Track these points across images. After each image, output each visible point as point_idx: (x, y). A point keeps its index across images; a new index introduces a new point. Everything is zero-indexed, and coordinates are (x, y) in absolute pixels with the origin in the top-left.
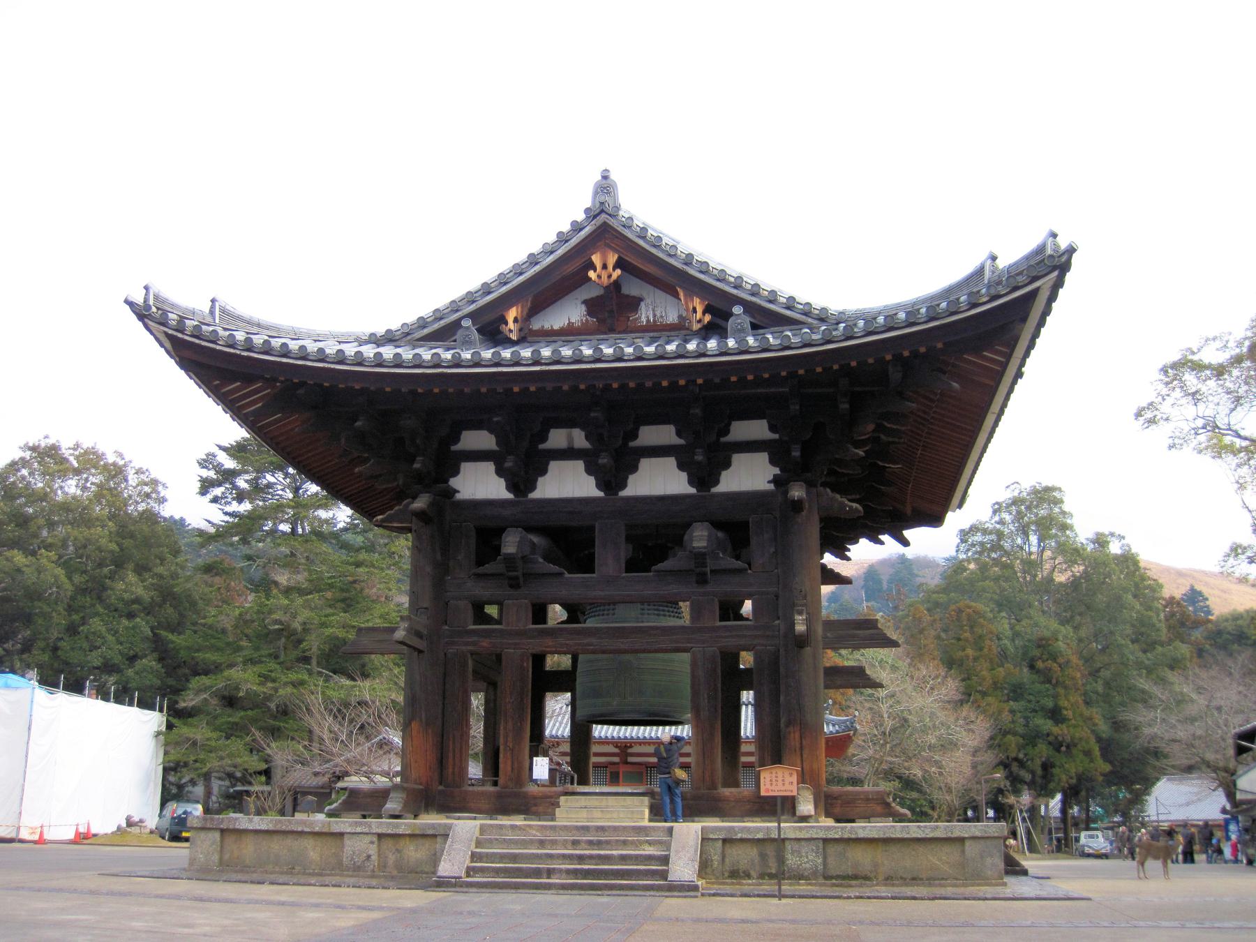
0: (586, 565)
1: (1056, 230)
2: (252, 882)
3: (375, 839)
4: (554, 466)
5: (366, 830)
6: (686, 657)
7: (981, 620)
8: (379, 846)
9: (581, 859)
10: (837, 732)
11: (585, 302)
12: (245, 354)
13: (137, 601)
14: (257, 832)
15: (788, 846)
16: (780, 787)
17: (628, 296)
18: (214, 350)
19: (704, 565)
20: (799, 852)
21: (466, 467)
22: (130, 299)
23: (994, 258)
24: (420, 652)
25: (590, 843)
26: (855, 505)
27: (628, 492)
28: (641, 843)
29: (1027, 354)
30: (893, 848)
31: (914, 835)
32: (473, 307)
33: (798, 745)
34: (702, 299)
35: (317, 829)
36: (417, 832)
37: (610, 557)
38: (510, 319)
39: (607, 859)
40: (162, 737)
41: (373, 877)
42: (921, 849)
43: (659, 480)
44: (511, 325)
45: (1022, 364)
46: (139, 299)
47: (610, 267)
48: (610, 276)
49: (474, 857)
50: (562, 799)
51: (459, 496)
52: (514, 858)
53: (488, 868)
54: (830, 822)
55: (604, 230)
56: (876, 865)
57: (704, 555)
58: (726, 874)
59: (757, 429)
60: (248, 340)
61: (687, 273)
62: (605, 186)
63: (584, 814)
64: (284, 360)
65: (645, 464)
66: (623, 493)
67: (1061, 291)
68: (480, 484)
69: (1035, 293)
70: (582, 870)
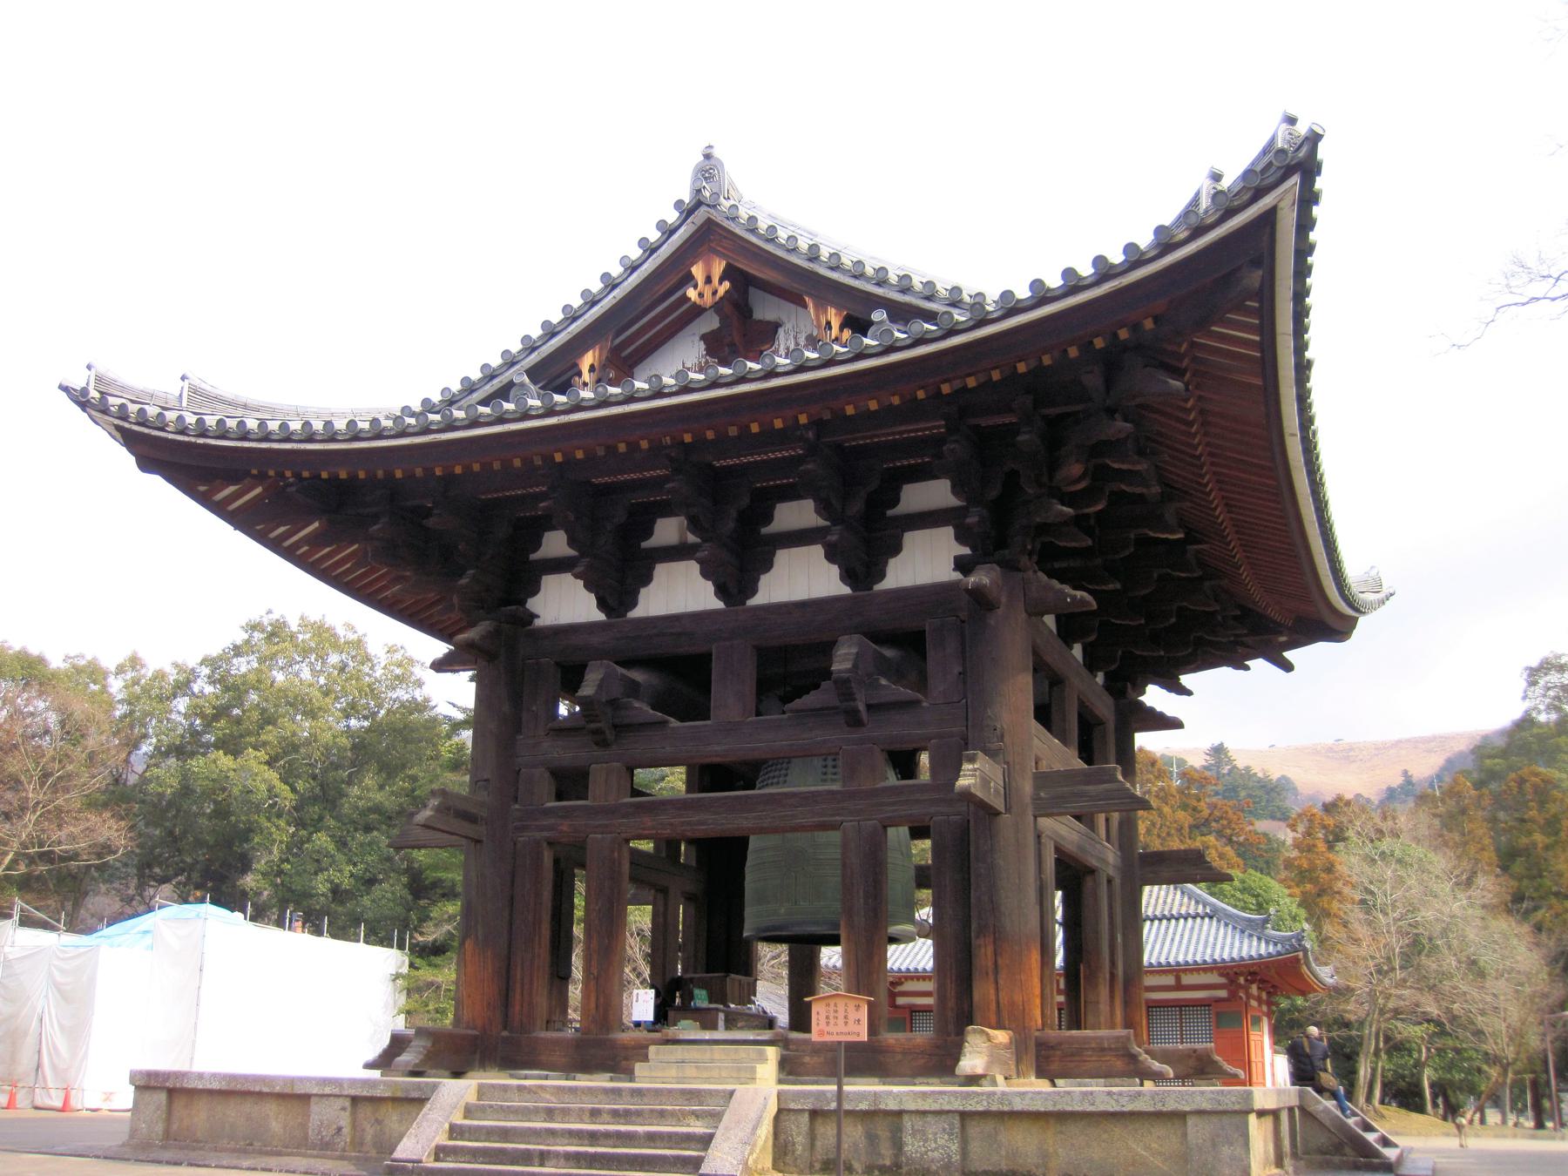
0: (698, 710)
1: (1293, 112)
2: (168, 1163)
3: (347, 1104)
4: (661, 570)
5: (337, 1091)
6: (835, 836)
7: (1555, 792)
8: (353, 1114)
9: (593, 1137)
10: (1279, 954)
11: (704, 338)
12: (201, 441)
13: (377, 809)
14: (210, 1092)
15: (907, 1123)
16: (841, 1028)
18: (166, 440)
19: (848, 695)
20: (924, 1133)
21: (550, 583)
22: (65, 384)
23: (1217, 177)
24: (478, 841)
25: (615, 1114)
26: (1079, 594)
27: (758, 600)
28: (685, 1114)
29: (1300, 328)
30: (1073, 1128)
31: (1102, 1108)
32: (534, 358)
33: (990, 964)
34: (838, 307)
35: (278, 1089)
36: (399, 1094)
37: (731, 694)
38: (585, 368)
39: (628, 1138)
40: (400, 982)
41: (342, 1158)
42: (1117, 1130)
43: (802, 578)
44: (586, 376)
45: (1301, 347)
46: (78, 383)
47: (716, 280)
48: (715, 293)
49: (455, 1131)
50: (652, 1049)
51: (538, 623)
52: (505, 1134)
53: (462, 1148)
54: (1043, 1086)
55: (706, 230)
56: (1045, 1156)
57: (847, 681)
58: (818, 1166)
59: (935, 493)
60: (200, 422)
61: (817, 274)
62: (708, 168)
63: (673, 1072)
64: (247, 444)
65: (783, 557)
66: (752, 602)
67: (1316, 210)
68: (565, 603)
69: (1270, 216)
70: (586, 1154)
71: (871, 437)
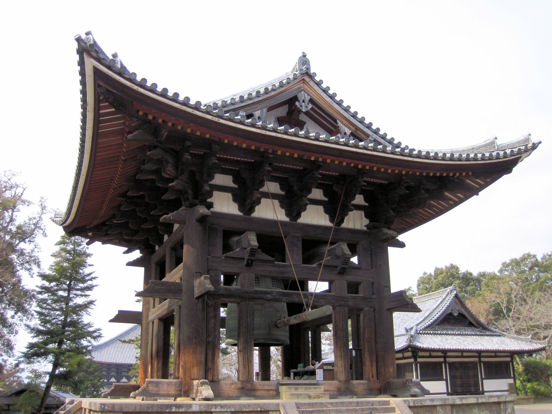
62: (304, 60)
68: (224, 205)
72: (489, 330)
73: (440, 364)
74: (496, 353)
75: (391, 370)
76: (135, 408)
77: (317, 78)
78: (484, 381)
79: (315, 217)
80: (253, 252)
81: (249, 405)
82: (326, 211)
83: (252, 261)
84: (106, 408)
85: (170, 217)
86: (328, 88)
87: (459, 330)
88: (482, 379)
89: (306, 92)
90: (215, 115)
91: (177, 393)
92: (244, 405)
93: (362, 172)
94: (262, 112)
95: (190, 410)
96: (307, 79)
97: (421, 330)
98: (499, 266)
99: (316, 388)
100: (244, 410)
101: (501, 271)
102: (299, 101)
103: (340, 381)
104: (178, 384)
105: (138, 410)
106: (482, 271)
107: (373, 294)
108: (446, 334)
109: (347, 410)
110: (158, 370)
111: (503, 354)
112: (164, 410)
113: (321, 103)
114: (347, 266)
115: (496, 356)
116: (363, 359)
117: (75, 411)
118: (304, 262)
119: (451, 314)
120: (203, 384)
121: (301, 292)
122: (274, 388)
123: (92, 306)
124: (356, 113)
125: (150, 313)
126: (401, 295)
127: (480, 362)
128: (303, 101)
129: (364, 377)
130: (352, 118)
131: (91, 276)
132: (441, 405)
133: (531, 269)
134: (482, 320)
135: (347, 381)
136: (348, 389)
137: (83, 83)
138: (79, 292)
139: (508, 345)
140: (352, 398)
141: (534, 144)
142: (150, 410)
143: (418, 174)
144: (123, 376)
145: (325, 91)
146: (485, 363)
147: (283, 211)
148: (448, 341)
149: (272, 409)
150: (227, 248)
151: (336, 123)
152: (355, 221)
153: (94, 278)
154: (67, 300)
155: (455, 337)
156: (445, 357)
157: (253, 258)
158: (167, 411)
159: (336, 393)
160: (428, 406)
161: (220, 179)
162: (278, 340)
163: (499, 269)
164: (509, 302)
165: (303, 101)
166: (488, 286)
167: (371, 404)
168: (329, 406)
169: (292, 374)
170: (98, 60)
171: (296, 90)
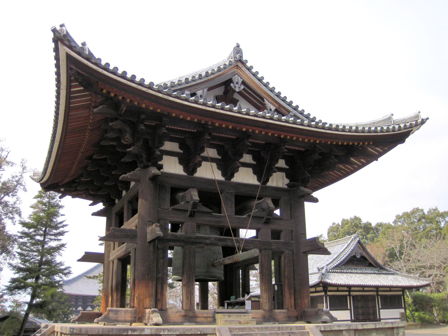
17: (235, 99)
62: (238, 50)
68: (172, 167)
71: (151, 123)
72: (386, 270)
73: (345, 296)
74: (390, 288)
75: (306, 301)
76: (99, 331)
77: (248, 65)
78: (381, 310)
79: (245, 177)
80: (195, 205)
81: (191, 329)
82: (255, 173)
83: (194, 212)
84: (75, 331)
85: (128, 176)
86: (257, 72)
87: (361, 269)
88: (379, 309)
89: (239, 76)
90: (165, 93)
91: (133, 319)
92: (187, 330)
93: (284, 141)
94: (203, 92)
95: (143, 333)
96: (240, 65)
97: (330, 269)
98: (393, 218)
99: (245, 316)
100: (187, 333)
101: (395, 222)
102: (233, 83)
103: (265, 310)
104: (133, 312)
105: (100, 333)
106: (379, 222)
107: (292, 240)
108: (351, 273)
109: (271, 333)
110: (117, 301)
111: (396, 289)
112: (121, 333)
113: (251, 85)
114: (271, 217)
115: (390, 291)
116: (284, 293)
117: (49, 333)
118: (236, 214)
119: (354, 257)
120: (153, 312)
121: (233, 238)
122: (212, 316)
123: (64, 248)
124: (280, 93)
125: (111, 255)
126: (315, 240)
127: (378, 295)
128: (237, 83)
129: (284, 307)
130: (276, 97)
131: (62, 224)
132: (346, 330)
133: (419, 220)
134: (380, 261)
135: (271, 310)
136: (271, 316)
137: (58, 66)
138: (53, 237)
139: (400, 282)
140: (275, 323)
141: (422, 120)
142: (110, 333)
143: (329, 143)
144: (88, 306)
145: (255, 75)
146: (381, 296)
147: (220, 172)
148: (352, 279)
149: (210, 333)
150: (174, 202)
151: (264, 101)
152: (278, 180)
153: (66, 226)
154: (43, 243)
155: (358, 275)
156: (349, 291)
157: (195, 210)
158: (124, 334)
159: (261, 320)
160: (336, 331)
161: (169, 146)
162: (214, 277)
163: (393, 220)
164: (402, 247)
165: (237, 83)
166: (385, 234)
167: (289, 329)
168: (256, 330)
169: (226, 304)
170: (70, 47)
171: (232, 73)
